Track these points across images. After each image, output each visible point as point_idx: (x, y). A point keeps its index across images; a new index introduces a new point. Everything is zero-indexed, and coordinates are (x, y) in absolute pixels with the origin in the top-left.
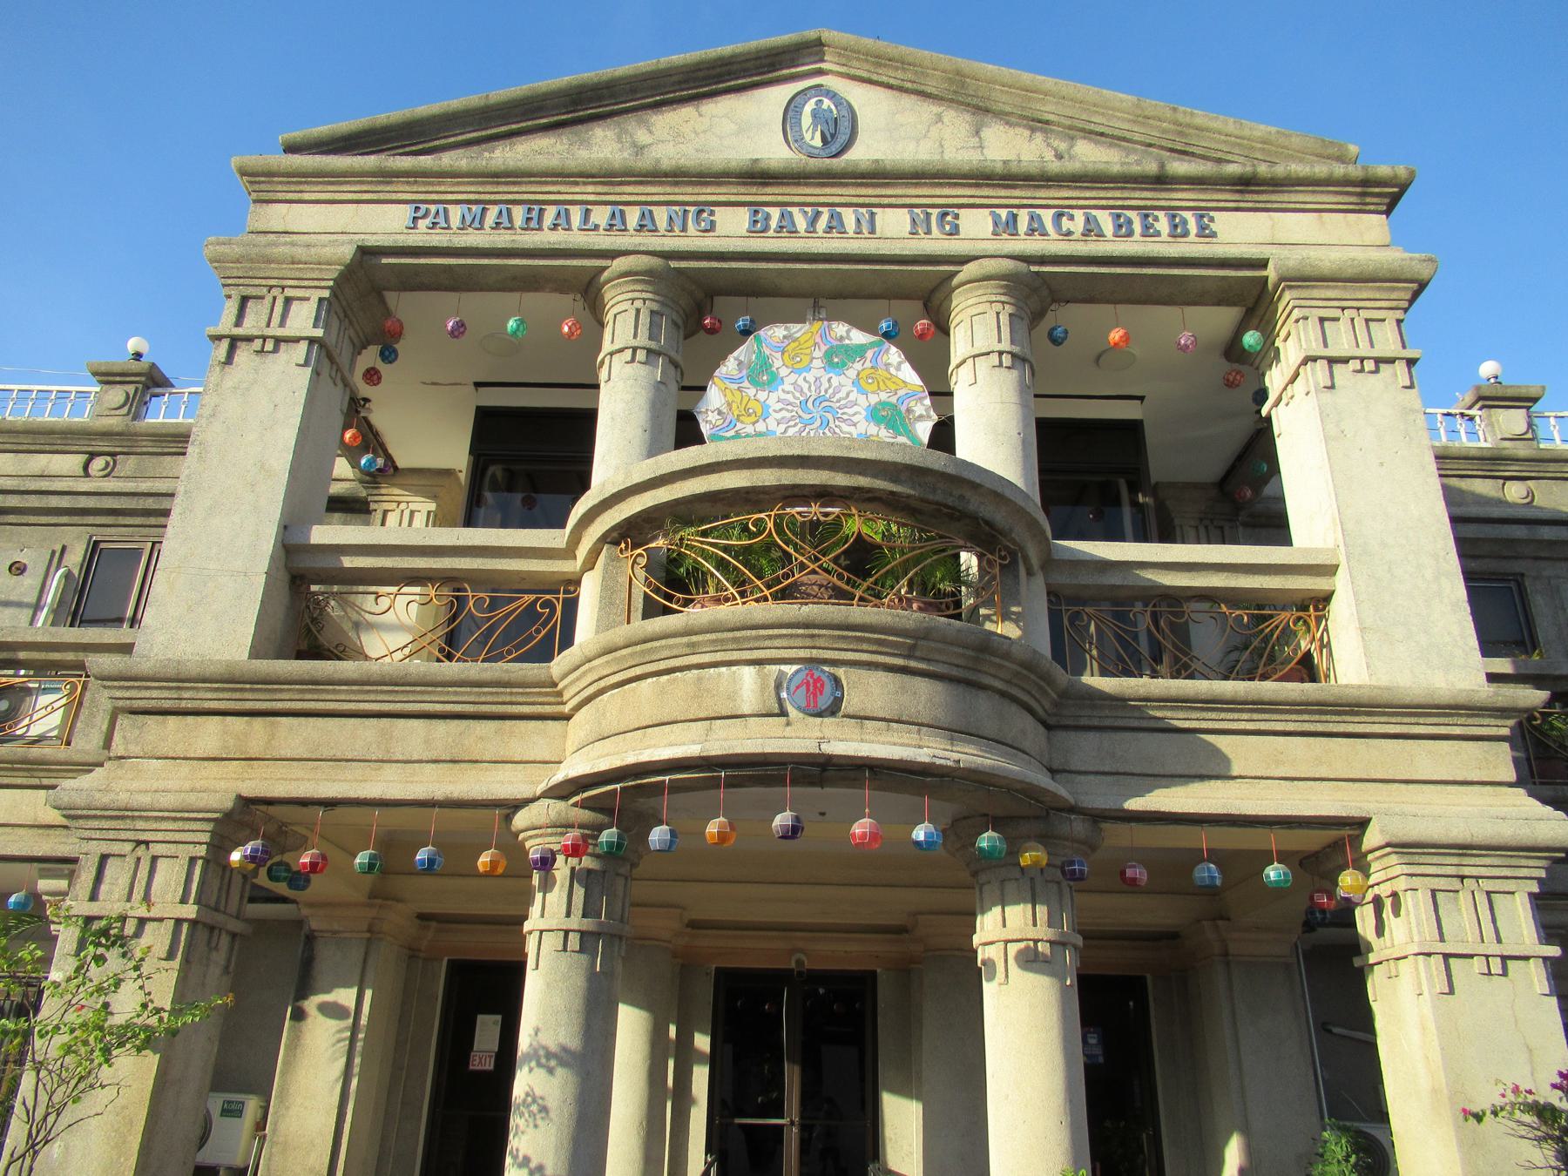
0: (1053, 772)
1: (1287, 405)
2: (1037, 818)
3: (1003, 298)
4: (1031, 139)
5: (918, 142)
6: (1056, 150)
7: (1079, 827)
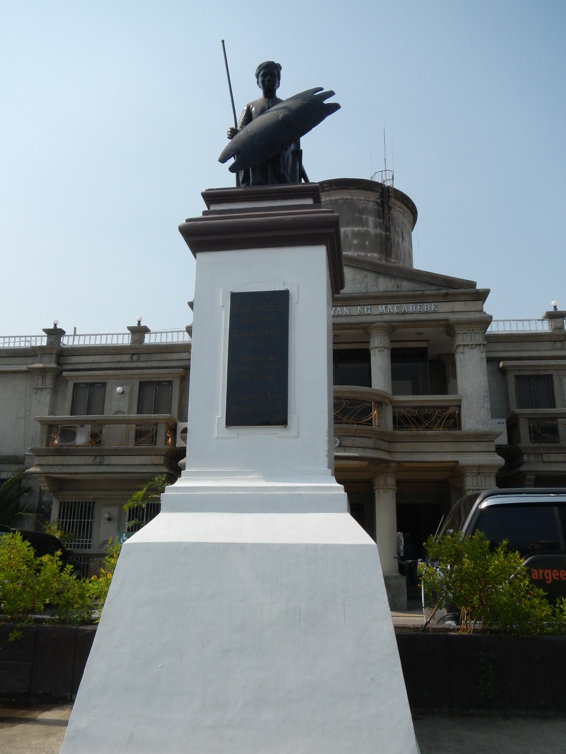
0: (390, 452)
3: (382, 332)
4: (390, 282)
5: (361, 284)
6: (397, 284)
7: (394, 465)
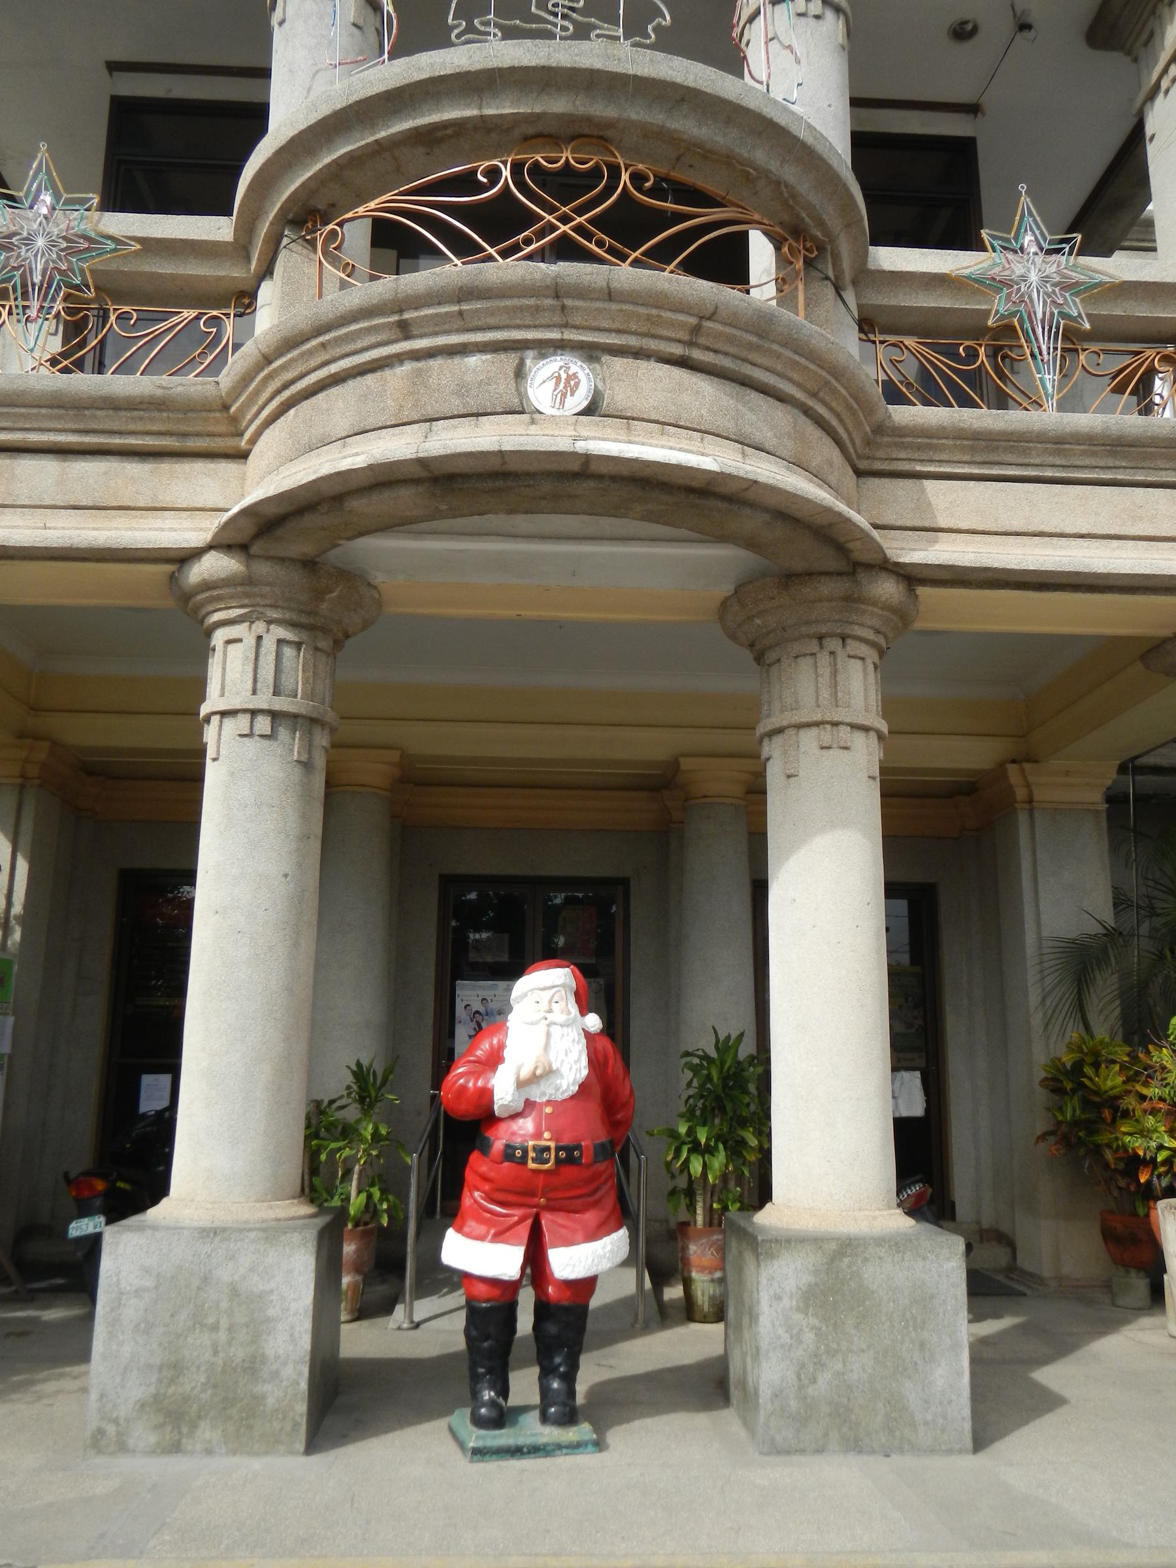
1: (1167, 92)
2: (840, 574)
7: (888, 589)
